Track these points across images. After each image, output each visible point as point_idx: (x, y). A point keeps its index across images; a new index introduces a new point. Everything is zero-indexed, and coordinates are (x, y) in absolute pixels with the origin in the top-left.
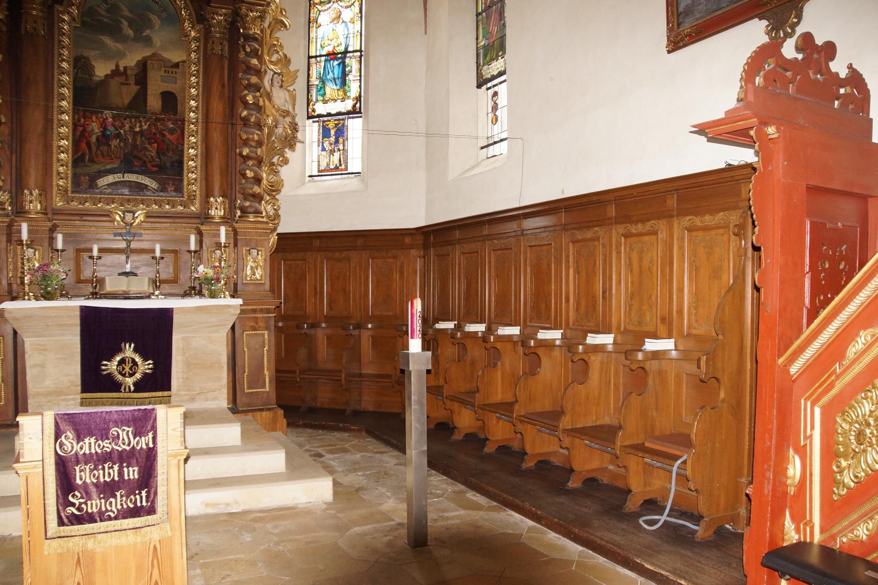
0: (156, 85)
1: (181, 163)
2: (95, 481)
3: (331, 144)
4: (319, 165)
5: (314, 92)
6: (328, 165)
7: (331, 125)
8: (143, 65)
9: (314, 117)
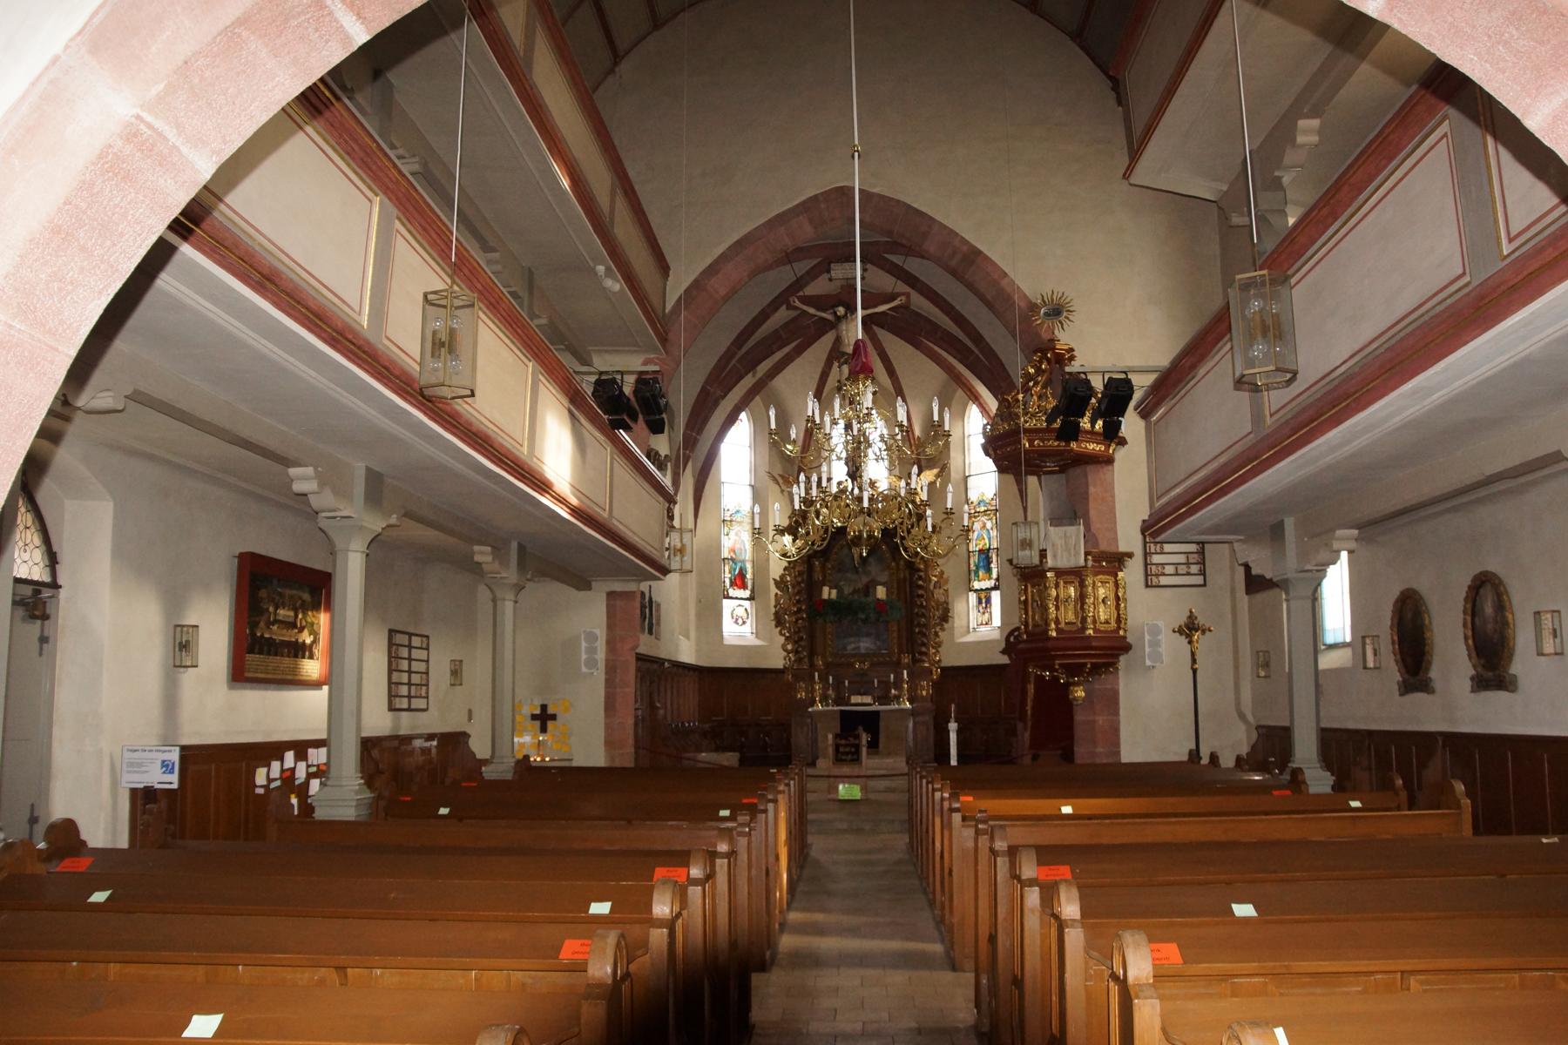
7: (983, 595)
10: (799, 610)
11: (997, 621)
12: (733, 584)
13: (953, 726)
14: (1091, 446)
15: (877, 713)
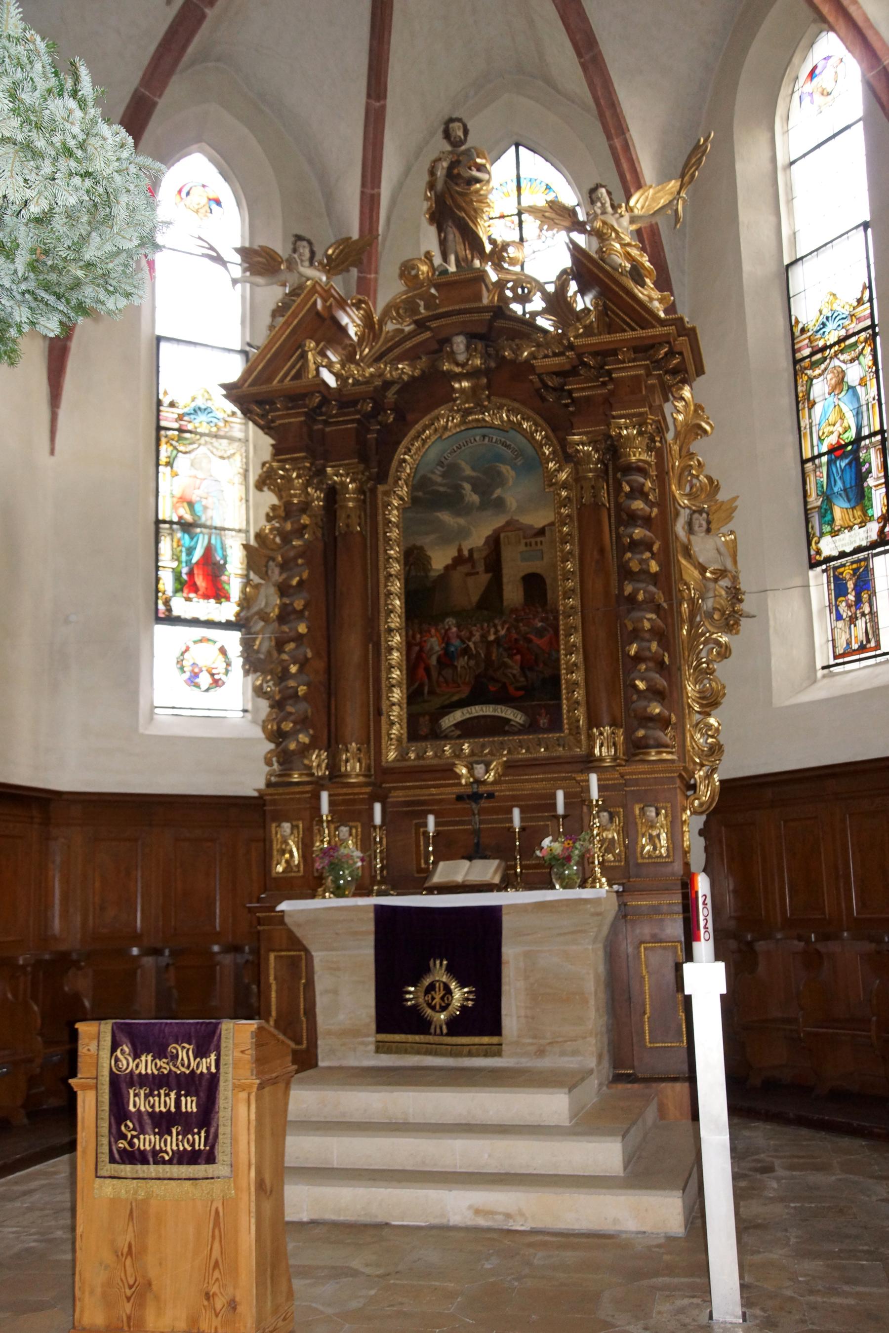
0: (514, 567)
1: (555, 680)
2: (150, 1110)
3: (849, 606)
4: (834, 647)
5: (815, 520)
6: (849, 643)
7: (847, 572)
8: (495, 543)
9: (819, 564)
15: (493, 915)
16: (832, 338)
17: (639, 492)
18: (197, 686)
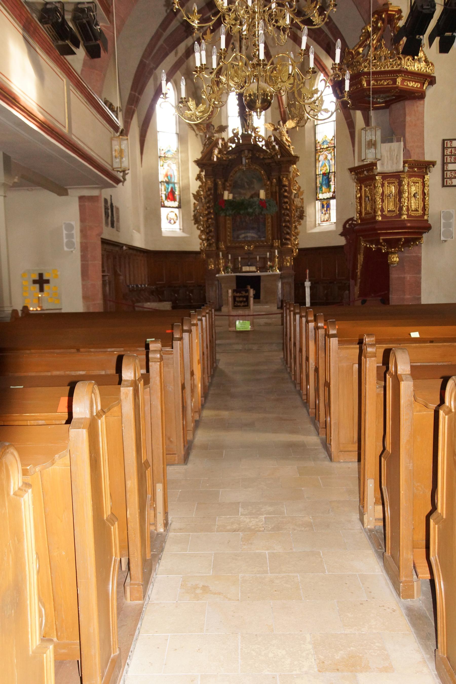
7: (325, 203)
10: (209, 213)
11: (334, 219)
12: (167, 198)
13: (307, 284)
14: (411, 84)
15: (259, 277)
16: (325, 146)
17: (286, 191)
18: (171, 223)
